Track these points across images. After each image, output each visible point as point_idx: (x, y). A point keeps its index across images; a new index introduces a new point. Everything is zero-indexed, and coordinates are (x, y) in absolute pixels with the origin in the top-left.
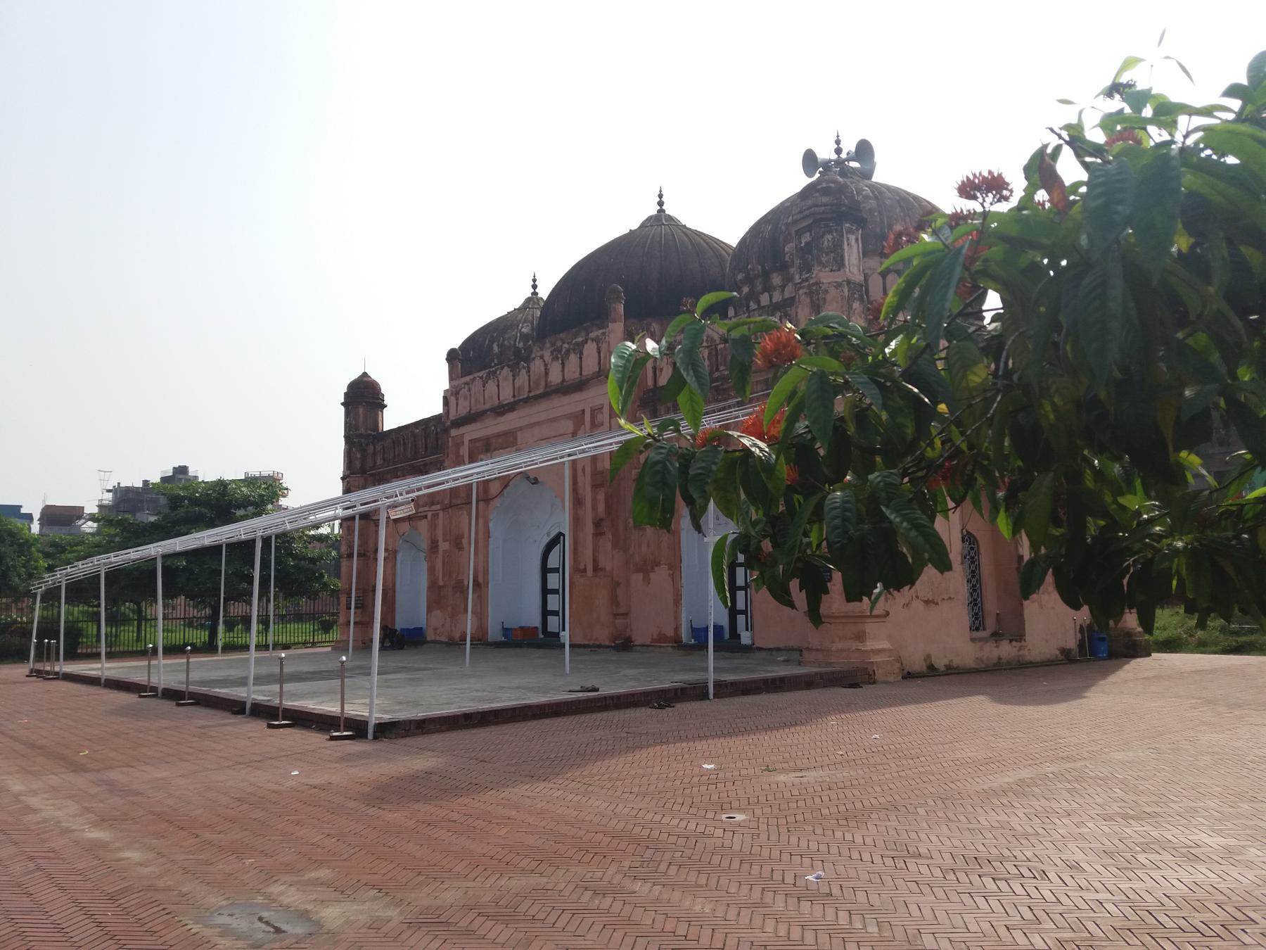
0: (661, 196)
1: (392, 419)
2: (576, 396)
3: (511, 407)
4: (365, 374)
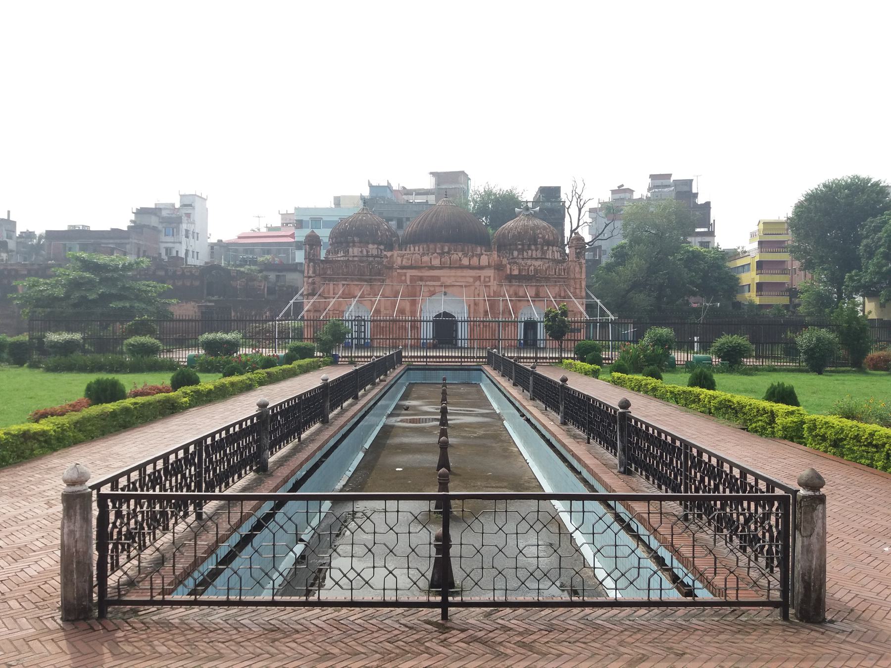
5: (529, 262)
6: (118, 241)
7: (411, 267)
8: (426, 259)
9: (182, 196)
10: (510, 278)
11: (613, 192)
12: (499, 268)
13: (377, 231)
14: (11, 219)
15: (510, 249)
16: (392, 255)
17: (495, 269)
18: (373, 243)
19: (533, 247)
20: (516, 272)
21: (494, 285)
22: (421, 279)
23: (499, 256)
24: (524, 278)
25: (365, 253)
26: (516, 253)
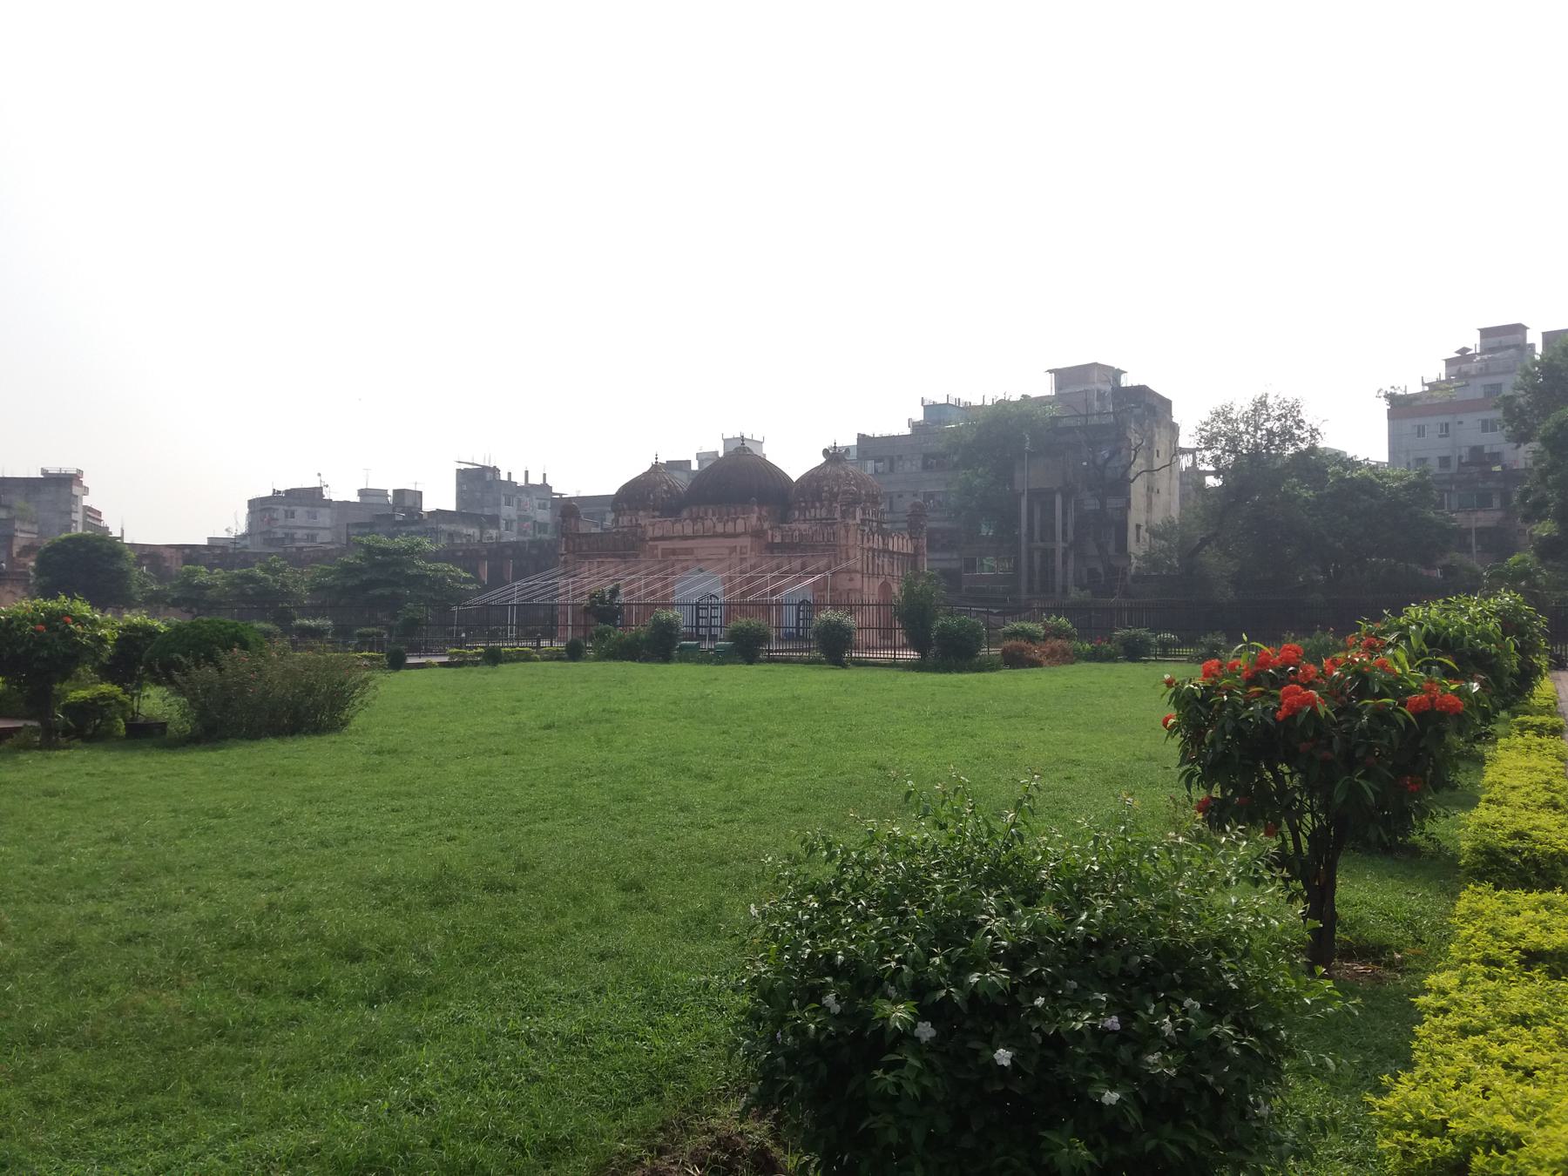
7: (663, 538)
8: (678, 526)
9: (726, 441)
10: (771, 547)
11: (1449, 362)
12: (758, 534)
20: (778, 540)
22: (674, 552)
24: (788, 547)
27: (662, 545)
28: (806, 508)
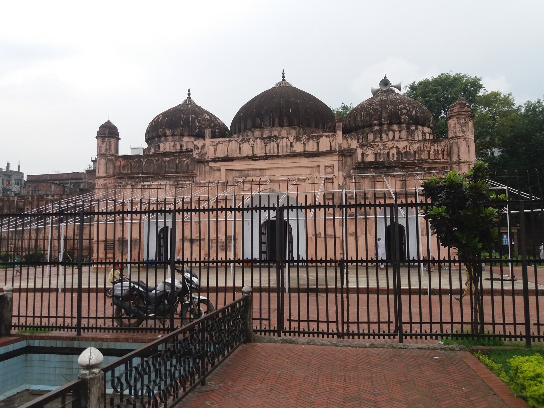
0: (283, 74)
1: (124, 149)
2: (315, 159)
3: (266, 158)
4: (109, 122)
5: (390, 144)
6: (75, 181)
7: (227, 159)
13: (193, 120)
14: (21, 171)
15: (363, 133)
16: (204, 145)
17: (339, 155)
18: (190, 135)
19: (395, 127)
20: (370, 158)
21: (339, 175)
23: (345, 138)
25: (178, 148)
26: (371, 137)
27: (225, 166)
28: (381, 132)
